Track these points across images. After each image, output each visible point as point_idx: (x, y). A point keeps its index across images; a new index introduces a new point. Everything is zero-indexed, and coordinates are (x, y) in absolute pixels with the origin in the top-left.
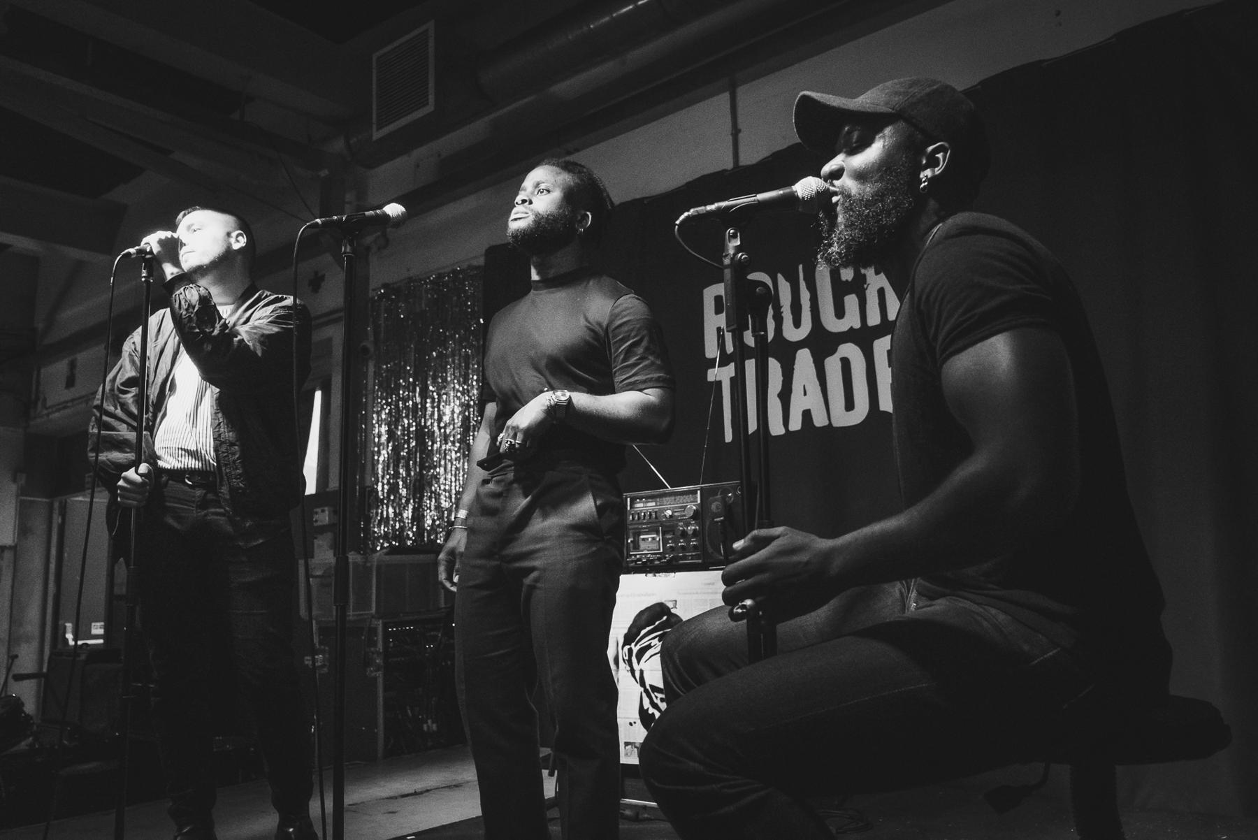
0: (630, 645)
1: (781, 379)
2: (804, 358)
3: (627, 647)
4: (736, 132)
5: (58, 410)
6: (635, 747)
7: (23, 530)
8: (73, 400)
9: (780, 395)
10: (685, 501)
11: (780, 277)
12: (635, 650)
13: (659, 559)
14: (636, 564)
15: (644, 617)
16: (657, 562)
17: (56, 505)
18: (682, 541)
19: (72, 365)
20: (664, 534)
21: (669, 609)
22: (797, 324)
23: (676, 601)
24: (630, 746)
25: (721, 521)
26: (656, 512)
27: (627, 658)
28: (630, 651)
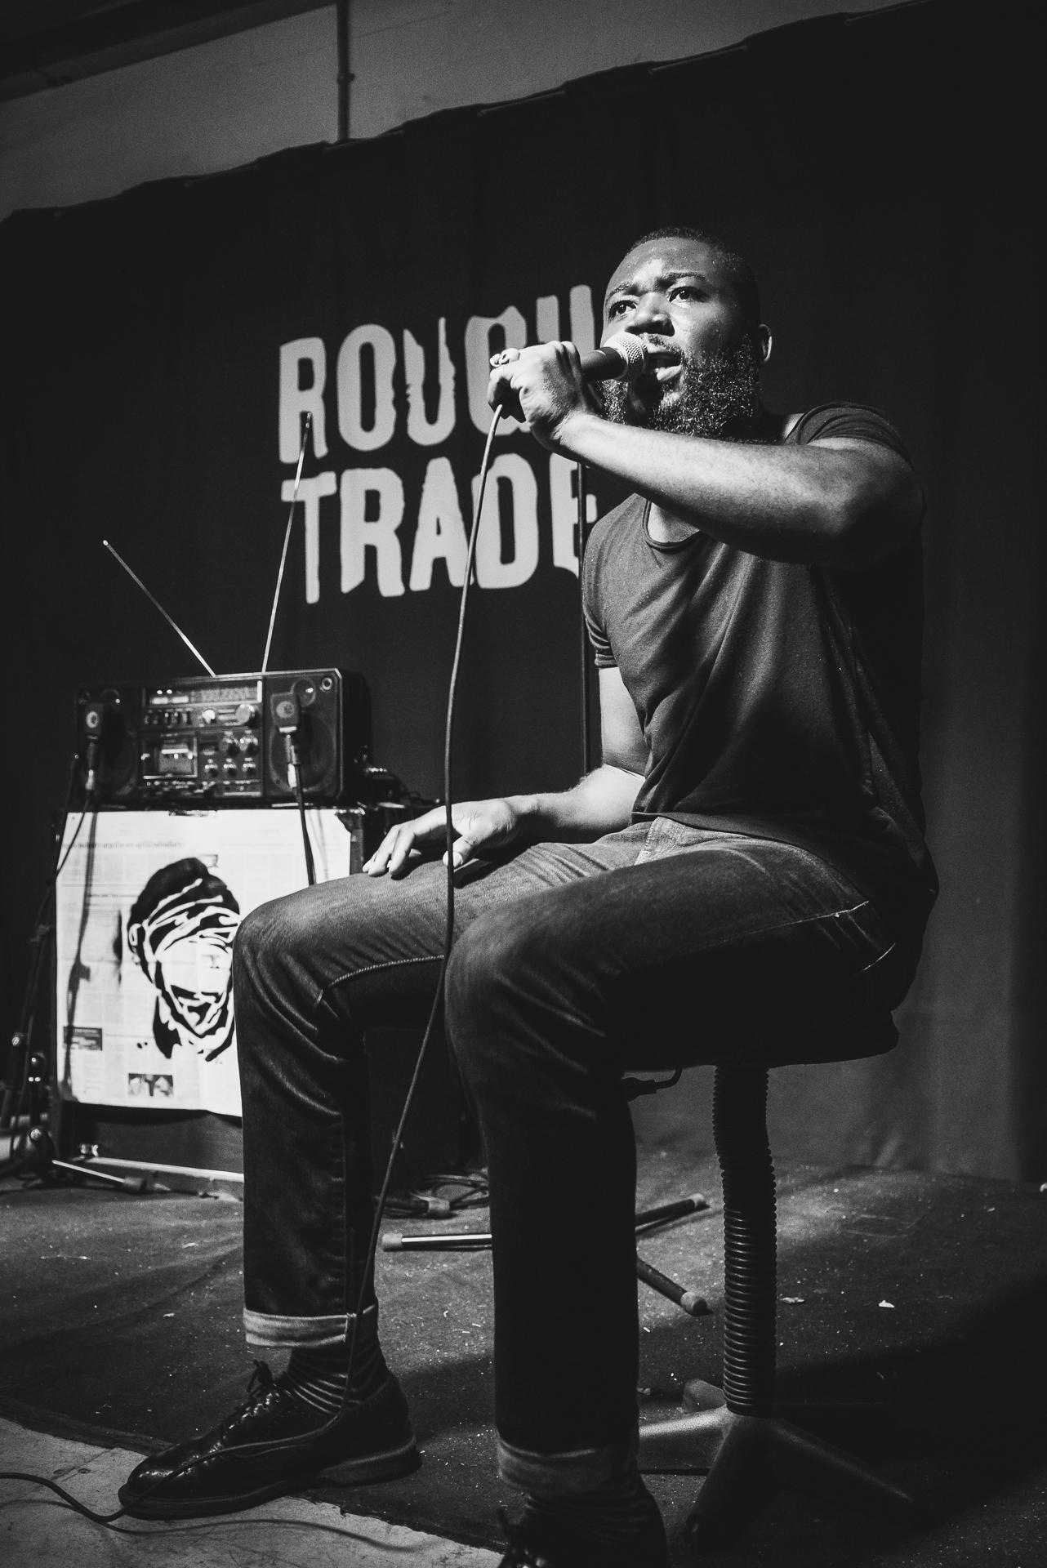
0: (141, 922)
1: (401, 504)
2: (440, 475)
3: (136, 926)
4: (345, 79)
6: (146, 1081)
10: (237, 697)
11: (408, 336)
12: (149, 930)
13: (192, 788)
15: (165, 880)
16: (188, 794)
18: (229, 760)
20: (201, 748)
21: (205, 869)
22: (432, 416)
23: (217, 856)
24: (136, 1080)
25: (292, 734)
26: (188, 713)
27: (135, 943)
28: (141, 932)
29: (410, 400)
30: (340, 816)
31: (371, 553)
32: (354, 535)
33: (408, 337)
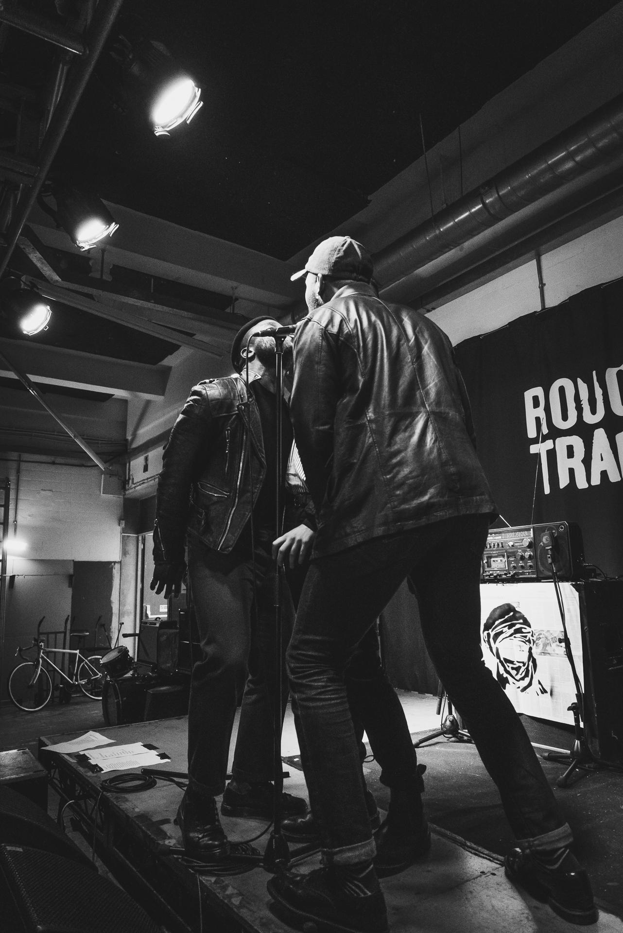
2: (600, 436)
3: (487, 632)
4: (542, 286)
5: (140, 485)
7: (125, 553)
8: (148, 479)
9: (582, 461)
10: (522, 535)
11: (579, 379)
12: (492, 634)
13: (506, 574)
14: (489, 577)
15: (498, 612)
16: (504, 576)
17: (140, 538)
18: (521, 562)
19: (146, 459)
20: (508, 557)
22: (594, 411)
26: (502, 543)
27: (486, 639)
28: (489, 635)
29: (582, 406)
30: (572, 585)
31: (571, 472)
32: (563, 465)
33: (579, 381)
